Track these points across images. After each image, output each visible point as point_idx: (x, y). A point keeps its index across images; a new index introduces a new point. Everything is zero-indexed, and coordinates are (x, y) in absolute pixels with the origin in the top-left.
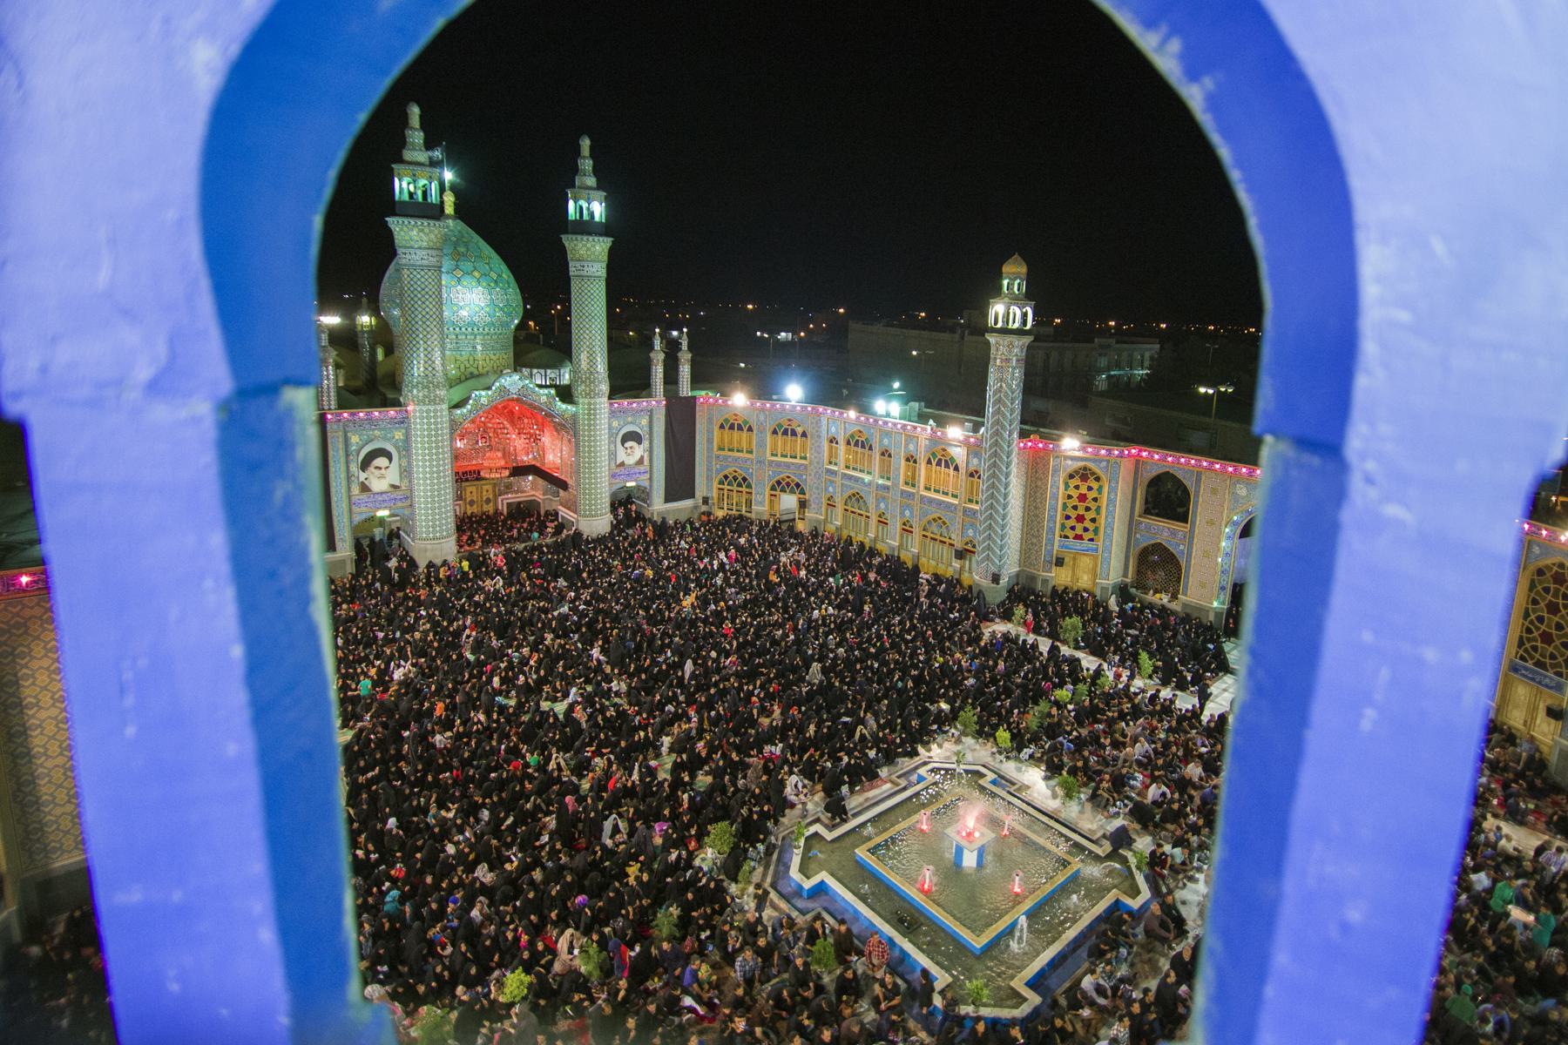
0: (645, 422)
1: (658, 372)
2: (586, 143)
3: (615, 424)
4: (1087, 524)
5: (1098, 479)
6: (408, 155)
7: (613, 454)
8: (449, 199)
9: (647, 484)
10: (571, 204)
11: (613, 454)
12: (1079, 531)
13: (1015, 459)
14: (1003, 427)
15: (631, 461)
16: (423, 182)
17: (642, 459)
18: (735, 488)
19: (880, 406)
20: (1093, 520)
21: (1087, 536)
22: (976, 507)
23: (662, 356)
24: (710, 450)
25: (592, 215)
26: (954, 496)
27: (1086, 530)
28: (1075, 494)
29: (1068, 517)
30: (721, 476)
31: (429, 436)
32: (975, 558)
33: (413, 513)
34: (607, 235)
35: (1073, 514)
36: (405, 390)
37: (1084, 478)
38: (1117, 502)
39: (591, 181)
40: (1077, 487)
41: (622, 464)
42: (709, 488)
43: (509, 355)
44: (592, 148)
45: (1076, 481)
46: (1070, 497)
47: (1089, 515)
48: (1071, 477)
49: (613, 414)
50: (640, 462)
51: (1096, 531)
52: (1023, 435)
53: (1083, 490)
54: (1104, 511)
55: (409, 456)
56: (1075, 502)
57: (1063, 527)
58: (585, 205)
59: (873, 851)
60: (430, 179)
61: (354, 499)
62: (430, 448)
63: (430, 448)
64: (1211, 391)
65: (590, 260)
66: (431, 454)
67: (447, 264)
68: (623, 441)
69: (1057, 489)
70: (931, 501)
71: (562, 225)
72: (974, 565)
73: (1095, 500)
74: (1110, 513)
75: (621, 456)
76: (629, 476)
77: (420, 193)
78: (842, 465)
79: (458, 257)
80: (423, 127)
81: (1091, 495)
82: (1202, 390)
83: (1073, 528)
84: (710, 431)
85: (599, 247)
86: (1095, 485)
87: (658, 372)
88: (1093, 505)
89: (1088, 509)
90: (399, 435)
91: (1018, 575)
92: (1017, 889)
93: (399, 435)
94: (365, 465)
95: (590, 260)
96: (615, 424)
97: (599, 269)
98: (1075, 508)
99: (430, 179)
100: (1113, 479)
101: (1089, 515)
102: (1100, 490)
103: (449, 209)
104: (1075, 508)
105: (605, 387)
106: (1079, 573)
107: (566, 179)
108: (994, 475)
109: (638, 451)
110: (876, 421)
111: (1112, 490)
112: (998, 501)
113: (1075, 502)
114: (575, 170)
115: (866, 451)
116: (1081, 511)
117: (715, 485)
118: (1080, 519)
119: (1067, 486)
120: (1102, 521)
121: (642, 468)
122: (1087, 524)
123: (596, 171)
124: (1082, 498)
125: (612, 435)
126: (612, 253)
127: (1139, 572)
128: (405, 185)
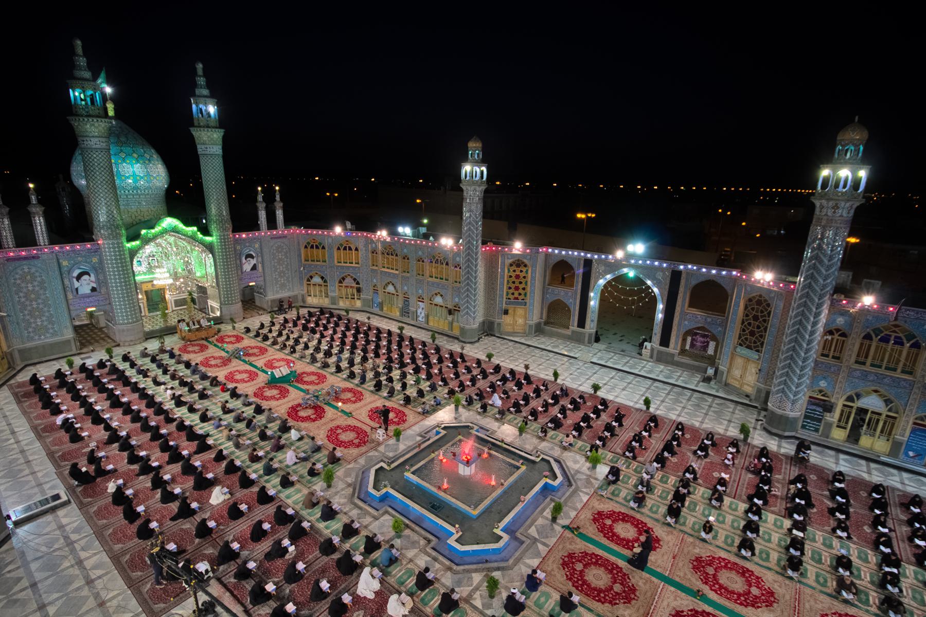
0: (257, 246)
1: (262, 215)
2: (200, 66)
3: (238, 247)
4: (521, 291)
5: (525, 266)
8: (110, 107)
9: (262, 283)
10: (194, 106)
12: (516, 295)
13: (480, 256)
14: (473, 238)
16: (90, 92)
19: (400, 229)
20: (524, 289)
21: (520, 298)
22: (397, 272)
23: (264, 205)
25: (209, 114)
26: (447, 280)
27: (520, 294)
28: (513, 274)
29: (510, 288)
30: (308, 276)
31: (116, 259)
32: (461, 313)
33: (112, 308)
34: (220, 127)
35: (513, 286)
36: (95, 231)
37: (518, 266)
38: (536, 277)
39: (205, 92)
40: (514, 271)
43: (162, 207)
45: (514, 268)
46: (511, 277)
47: (521, 286)
48: (511, 265)
51: (525, 295)
52: (484, 243)
53: (518, 273)
54: (529, 283)
55: (104, 273)
56: (513, 279)
57: (507, 294)
58: (204, 108)
59: (413, 473)
60: (95, 90)
61: (70, 302)
62: (118, 267)
63: (118, 267)
64: (583, 216)
65: (210, 144)
66: (118, 271)
67: (113, 149)
69: (504, 272)
70: (433, 283)
71: (188, 120)
72: (460, 318)
73: (524, 277)
74: (533, 285)
77: (88, 99)
78: (381, 266)
79: (120, 143)
81: (522, 275)
82: (579, 216)
83: (513, 294)
85: (217, 135)
86: (524, 270)
87: (262, 215)
88: (523, 281)
89: (521, 283)
90: (95, 260)
91: (484, 322)
92: (493, 483)
93: (95, 260)
94: (78, 278)
95: (210, 144)
97: (217, 150)
98: (514, 282)
99: (95, 90)
100: (534, 266)
101: (521, 286)
102: (527, 272)
103: (111, 113)
104: (514, 282)
106: (517, 319)
107: (190, 90)
108: (468, 266)
110: (399, 239)
111: (534, 272)
112: (471, 281)
113: (513, 279)
114: (195, 85)
115: (394, 257)
116: (517, 284)
118: (517, 288)
119: (509, 271)
120: (528, 289)
122: (521, 291)
123: (209, 86)
124: (517, 277)
126: (225, 139)
127: (548, 316)
128: (77, 94)
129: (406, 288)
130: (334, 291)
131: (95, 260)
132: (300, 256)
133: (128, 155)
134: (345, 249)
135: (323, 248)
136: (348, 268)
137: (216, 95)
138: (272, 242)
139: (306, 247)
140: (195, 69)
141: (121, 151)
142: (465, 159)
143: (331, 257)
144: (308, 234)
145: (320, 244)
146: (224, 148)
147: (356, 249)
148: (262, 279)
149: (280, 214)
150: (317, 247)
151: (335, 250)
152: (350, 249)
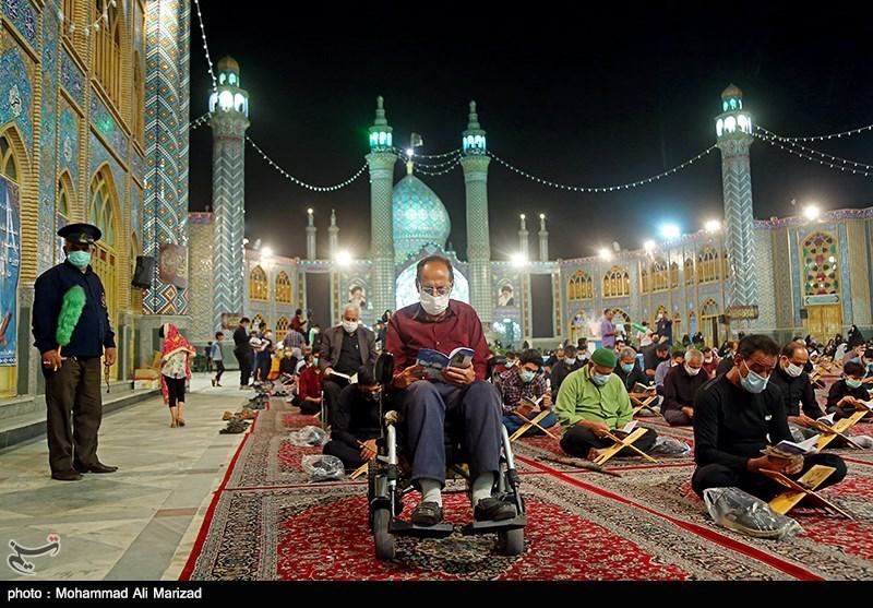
2: (473, 104)
6: (377, 122)
24: (564, 300)
37: (818, 242)
39: (477, 125)
44: (477, 107)
49: (493, 271)
80: (385, 107)
95: (477, 174)
105: (487, 253)
129: (676, 308)
133: (417, 202)
135: (590, 279)
137: (486, 126)
139: (572, 282)
140: (469, 108)
141: (410, 199)
142: (719, 112)
144: (574, 265)
146: (488, 177)
147: (626, 275)
149: (544, 243)
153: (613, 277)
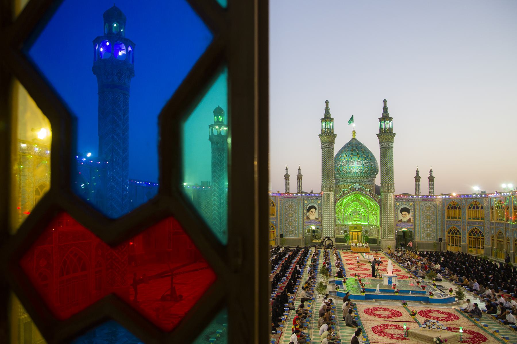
0: (411, 204)
7: (396, 216)
9: (412, 230)
11: (396, 216)
15: (405, 220)
17: (410, 219)
18: (454, 235)
30: (448, 230)
41: (401, 221)
42: (444, 236)
50: (409, 220)
68: (401, 212)
75: (401, 217)
76: (404, 226)
84: (444, 210)
96: (398, 204)
109: (408, 216)
117: (446, 234)
121: (410, 223)
125: (396, 209)
130: (465, 241)
131: (319, 202)
132: (444, 214)
134: (474, 208)
135: (460, 208)
136: (475, 223)
138: (423, 203)
139: (448, 208)
143: (464, 214)
145: (458, 205)
147: (482, 208)
148: (413, 227)
150: (456, 208)
151: (467, 209)
152: (478, 208)
153: (474, 208)
